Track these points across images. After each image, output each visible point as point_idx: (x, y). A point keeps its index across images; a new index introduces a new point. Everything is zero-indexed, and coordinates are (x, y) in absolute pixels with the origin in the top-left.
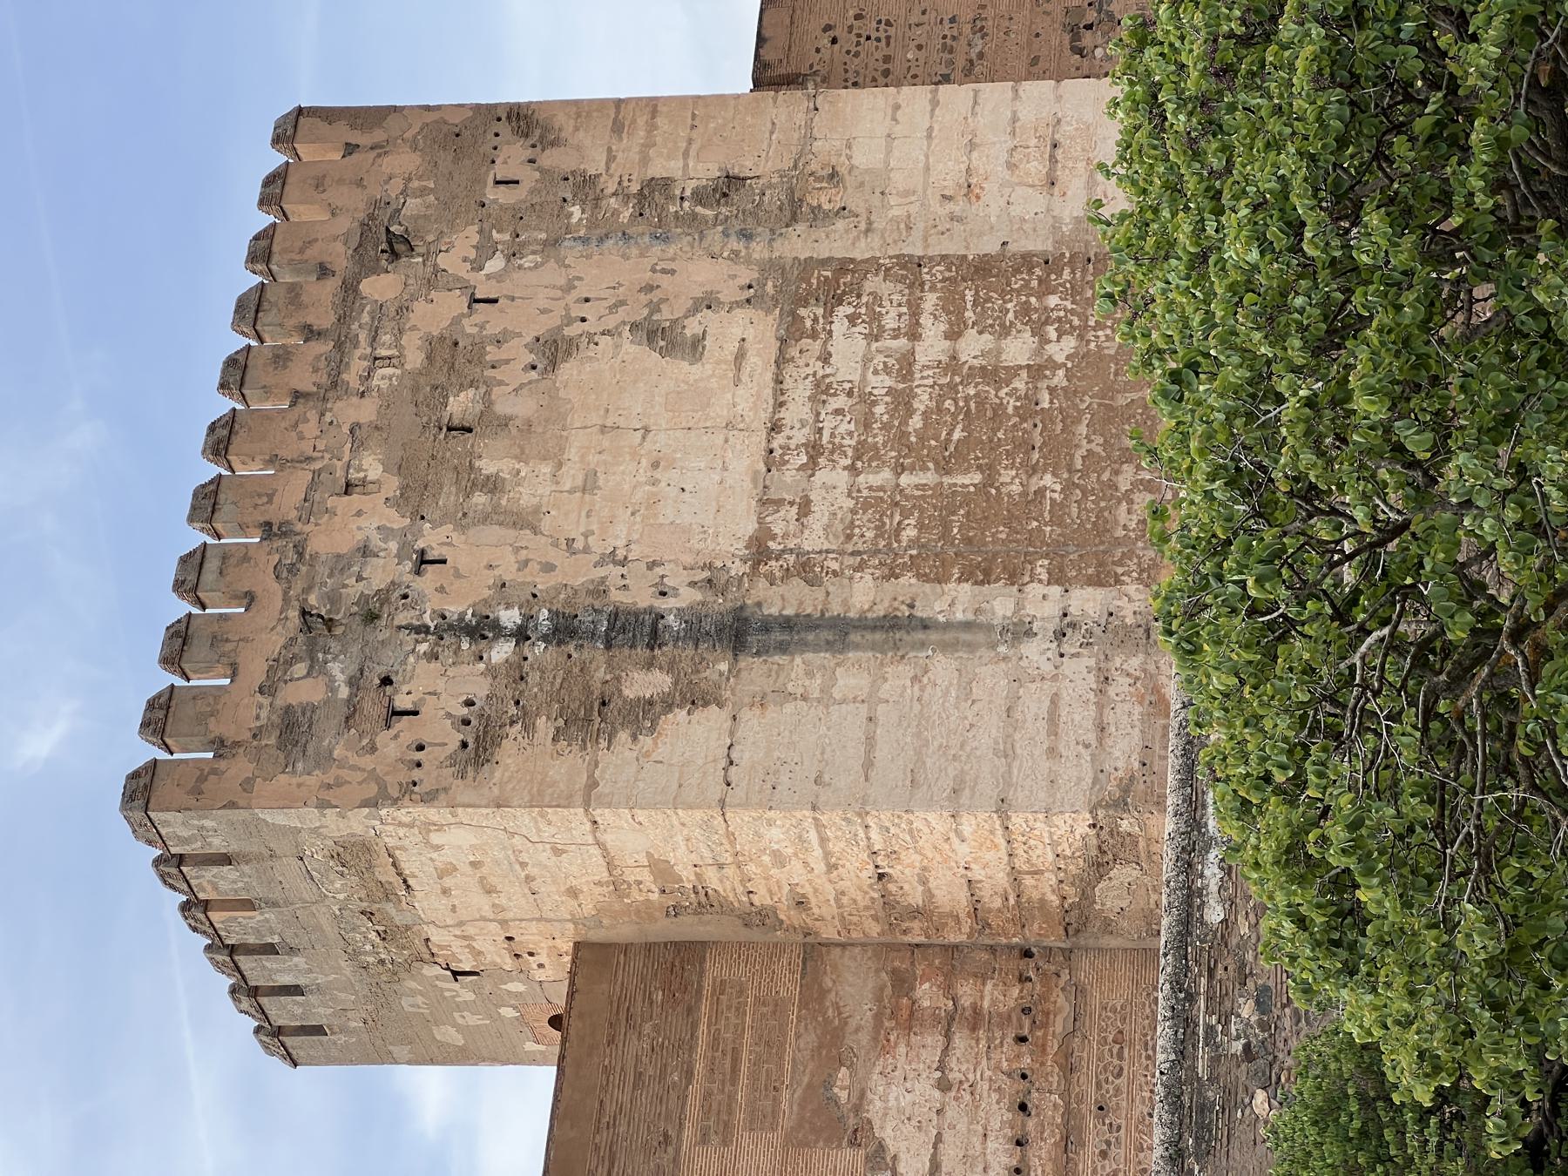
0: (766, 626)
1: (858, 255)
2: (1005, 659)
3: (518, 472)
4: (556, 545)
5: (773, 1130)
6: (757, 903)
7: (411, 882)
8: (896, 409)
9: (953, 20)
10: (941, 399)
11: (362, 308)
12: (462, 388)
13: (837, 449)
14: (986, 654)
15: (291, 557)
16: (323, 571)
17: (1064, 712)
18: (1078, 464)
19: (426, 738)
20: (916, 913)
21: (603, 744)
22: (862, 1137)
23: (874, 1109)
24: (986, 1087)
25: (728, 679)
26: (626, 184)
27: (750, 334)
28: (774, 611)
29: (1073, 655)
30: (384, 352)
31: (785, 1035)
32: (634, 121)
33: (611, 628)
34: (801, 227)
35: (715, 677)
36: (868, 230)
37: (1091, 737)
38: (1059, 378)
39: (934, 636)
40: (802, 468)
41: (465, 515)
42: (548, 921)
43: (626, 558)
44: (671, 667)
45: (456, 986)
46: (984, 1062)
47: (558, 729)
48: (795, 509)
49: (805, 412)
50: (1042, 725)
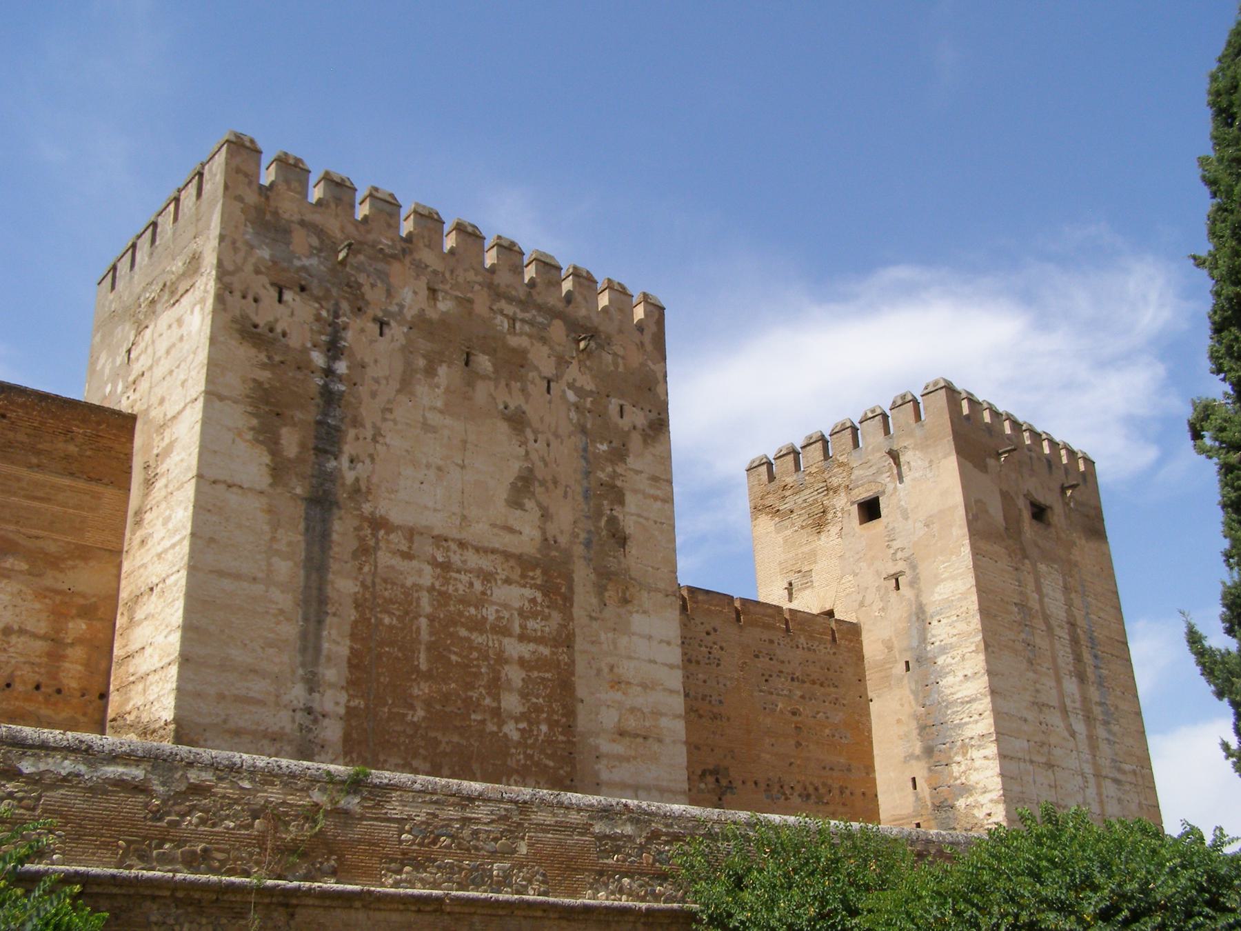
0: (326, 521)
2: (293, 672)
3: (438, 388)
4: (389, 401)
7: (177, 305)
9: (721, 702)
11: (546, 319)
12: (494, 365)
14: (299, 659)
16: (381, 266)
18: (432, 734)
20: (131, 619)
21: (249, 409)
25: (290, 492)
26: (621, 478)
30: (518, 325)
32: (659, 488)
34: (593, 576)
36: (591, 618)
38: (491, 727)
40: (434, 558)
41: (411, 352)
43: (377, 442)
48: (405, 549)
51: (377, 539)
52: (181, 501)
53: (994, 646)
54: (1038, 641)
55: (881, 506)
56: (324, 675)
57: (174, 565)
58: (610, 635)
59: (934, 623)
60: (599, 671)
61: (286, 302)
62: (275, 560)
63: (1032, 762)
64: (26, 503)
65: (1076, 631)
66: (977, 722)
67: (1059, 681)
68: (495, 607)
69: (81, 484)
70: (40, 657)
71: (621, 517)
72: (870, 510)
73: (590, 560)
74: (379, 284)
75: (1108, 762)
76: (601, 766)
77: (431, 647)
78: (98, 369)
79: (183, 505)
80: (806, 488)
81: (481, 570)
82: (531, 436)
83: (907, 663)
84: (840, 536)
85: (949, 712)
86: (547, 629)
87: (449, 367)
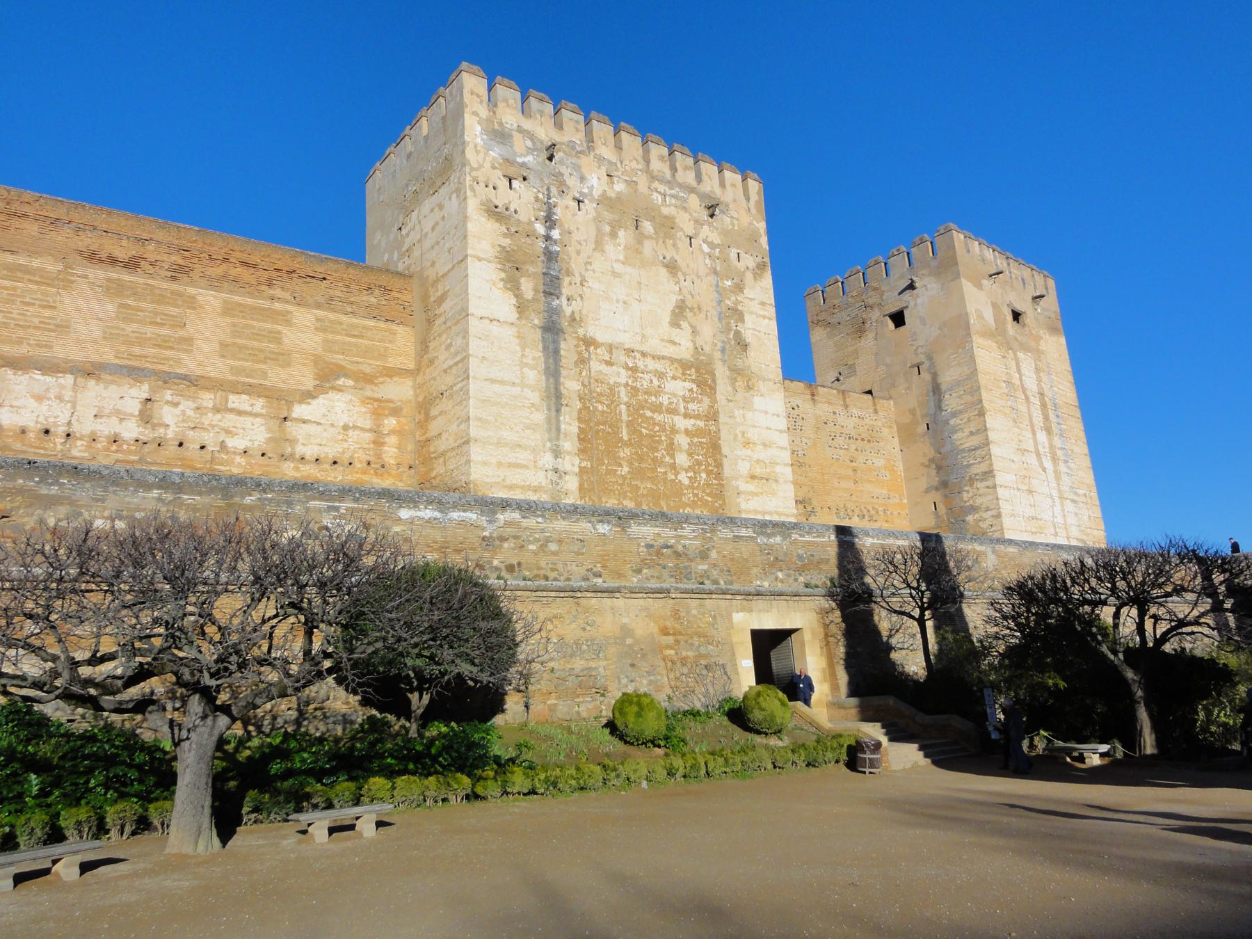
0: (556, 342)
4: (589, 257)
5: (324, 350)
6: (430, 344)
8: (654, 406)
10: (659, 425)
12: (654, 228)
13: (636, 380)
14: (547, 436)
15: (578, 149)
17: (520, 471)
18: (634, 483)
19: (498, 191)
21: (499, 266)
23: (332, 395)
24: (345, 446)
29: (546, 476)
30: (667, 199)
31: (370, 359)
32: (766, 310)
34: (728, 372)
35: (532, 318)
37: (508, 482)
39: (553, 413)
40: (626, 364)
44: (534, 300)
48: (608, 359)
50: (513, 460)
51: (589, 353)
52: (459, 333)
54: (1020, 407)
55: (906, 316)
56: (563, 446)
57: (459, 377)
58: (741, 411)
59: (947, 396)
60: (736, 435)
61: (515, 189)
62: (525, 370)
63: (1018, 489)
66: (980, 462)
67: (1034, 433)
69: (382, 325)
70: (369, 444)
71: (743, 332)
72: (898, 319)
73: (725, 361)
74: (575, 173)
75: (1067, 488)
76: (741, 500)
79: (461, 335)
80: (850, 307)
81: (656, 370)
82: (682, 278)
83: (928, 424)
84: (876, 339)
85: (959, 457)
87: (625, 231)
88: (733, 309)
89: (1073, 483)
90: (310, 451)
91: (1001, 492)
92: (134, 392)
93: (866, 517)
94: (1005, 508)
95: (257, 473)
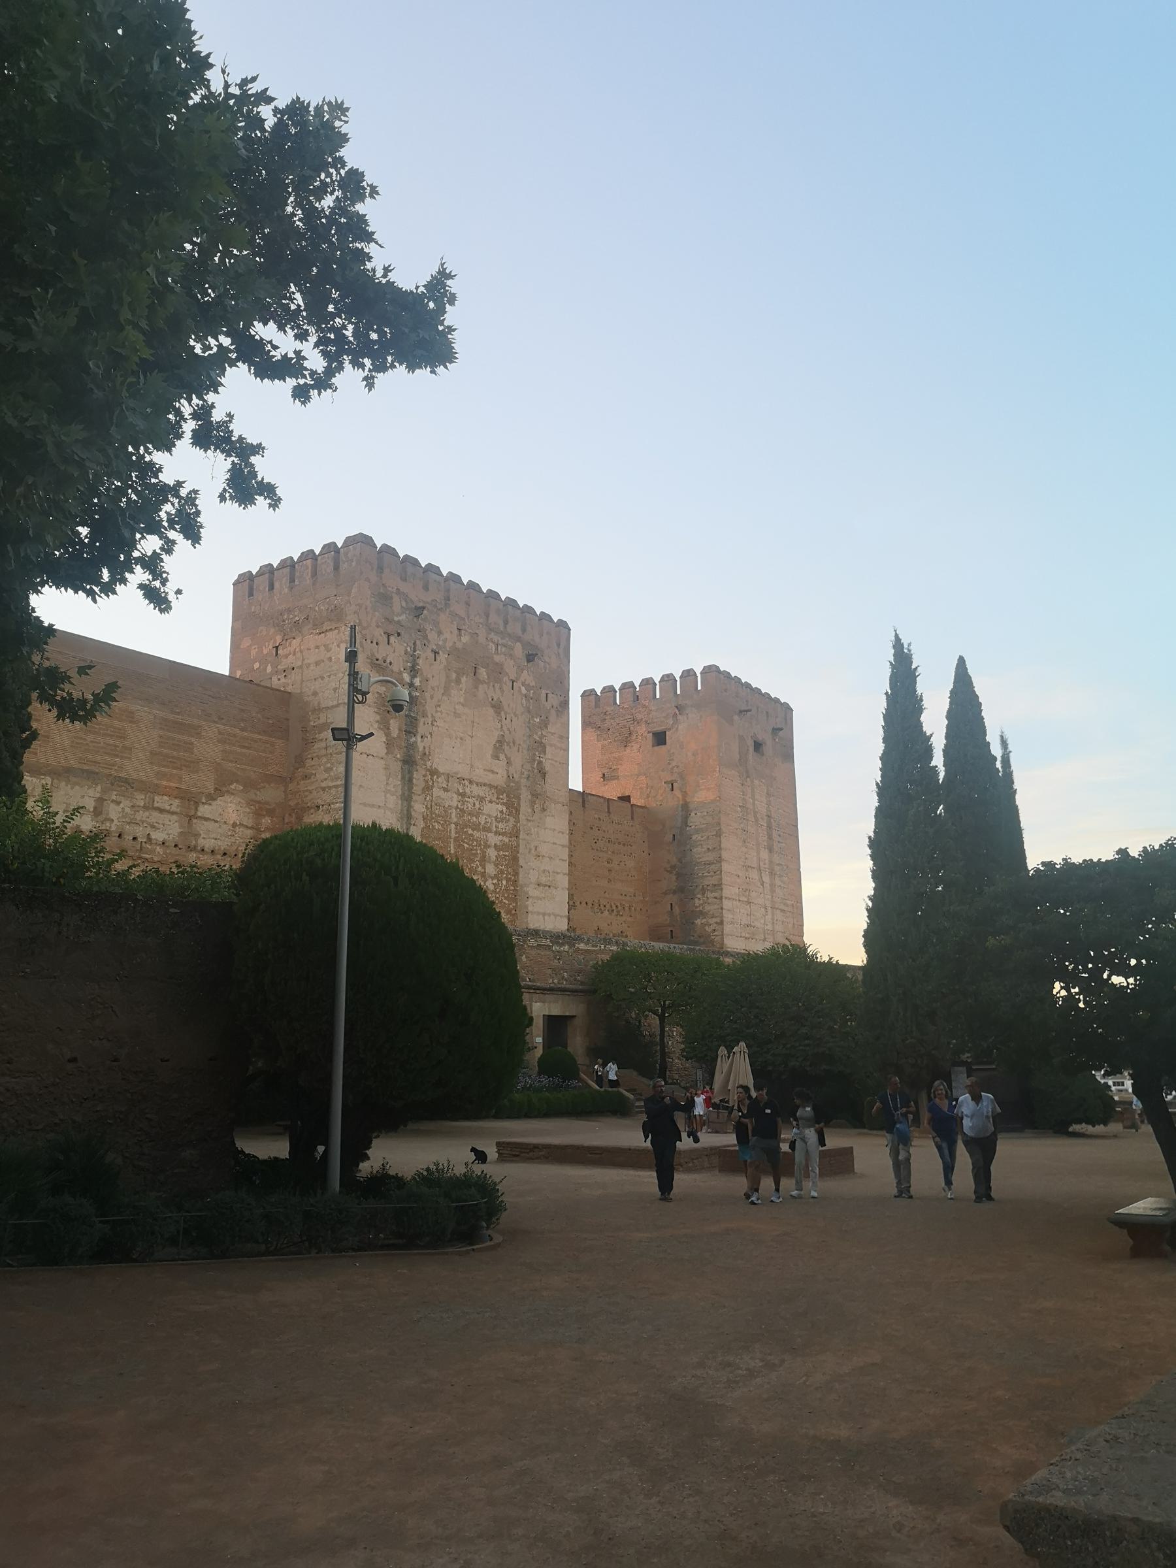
0: (410, 772)
1: (521, 816)
4: (439, 701)
7: (323, 635)
10: (477, 841)
12: (488, 674)
15: (439, 607)
21: (376, 710)
22: (219, 792)
23: (227, 798)
24: (233, 841)
27: (499, 776)
28: (415, 776)
33: (413, 718)
34: (530, 797)
40: (458, 790)
42: (301, 683)
44: (398, 737)
45: (271, 647)
46: (242, 841)
47: (381, 694)
48: (446, 786)
49: (475, 793)
53: (726, 833)
59: (693, 814)
63: (740, 900)
64: (239, 750)
65: (770, 820)
66: (712, 876)
67: (758, 853)
68: (485, 816)
71: (544, 761)
72: (660, 738)
76: (529, 903)
77: (456, 839)
78: (242, 647)
83: (674, 835)
84: (639, 751)
86: (507, 828)
88: (539, 742)
89: (784, 895)
90: (208, 843)
91: (727, 904)
92: (91, 792)
93: (615, 912)
94: (728, 917)
95: (170, 861)
